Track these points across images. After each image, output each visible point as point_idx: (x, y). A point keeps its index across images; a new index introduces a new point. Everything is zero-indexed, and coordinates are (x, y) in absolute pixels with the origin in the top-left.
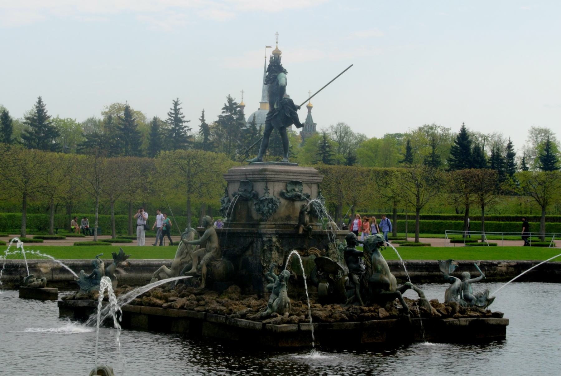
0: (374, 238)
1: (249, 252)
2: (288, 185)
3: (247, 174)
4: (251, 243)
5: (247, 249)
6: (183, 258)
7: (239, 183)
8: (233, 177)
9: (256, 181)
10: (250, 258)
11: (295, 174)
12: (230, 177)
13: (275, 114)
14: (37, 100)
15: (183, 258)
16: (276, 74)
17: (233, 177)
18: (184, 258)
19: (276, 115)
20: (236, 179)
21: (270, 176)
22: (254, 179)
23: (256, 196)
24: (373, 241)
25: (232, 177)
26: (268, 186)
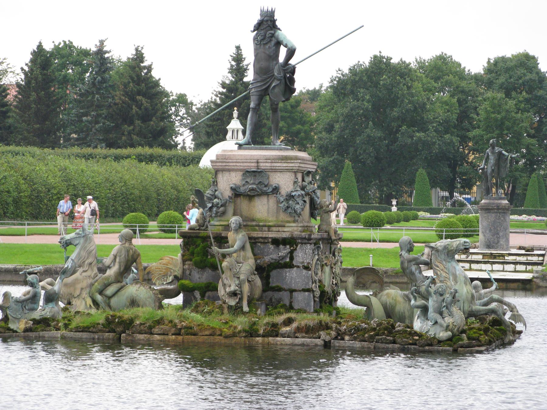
0: (458, 243)
2: (305, 175)
3: (260, 161)
6: (84, 271)
9: (275, 171)
11: (305, 162)
12: (224, 164)
13: (273, 85)
14: (234, 50)
16: (272, 32)
18: (86, 271)
19: (275, 86)
20: (236, 167)
21: (264, 164)
22: (272, 168)
24: (454, 246)
25: (227, 164)
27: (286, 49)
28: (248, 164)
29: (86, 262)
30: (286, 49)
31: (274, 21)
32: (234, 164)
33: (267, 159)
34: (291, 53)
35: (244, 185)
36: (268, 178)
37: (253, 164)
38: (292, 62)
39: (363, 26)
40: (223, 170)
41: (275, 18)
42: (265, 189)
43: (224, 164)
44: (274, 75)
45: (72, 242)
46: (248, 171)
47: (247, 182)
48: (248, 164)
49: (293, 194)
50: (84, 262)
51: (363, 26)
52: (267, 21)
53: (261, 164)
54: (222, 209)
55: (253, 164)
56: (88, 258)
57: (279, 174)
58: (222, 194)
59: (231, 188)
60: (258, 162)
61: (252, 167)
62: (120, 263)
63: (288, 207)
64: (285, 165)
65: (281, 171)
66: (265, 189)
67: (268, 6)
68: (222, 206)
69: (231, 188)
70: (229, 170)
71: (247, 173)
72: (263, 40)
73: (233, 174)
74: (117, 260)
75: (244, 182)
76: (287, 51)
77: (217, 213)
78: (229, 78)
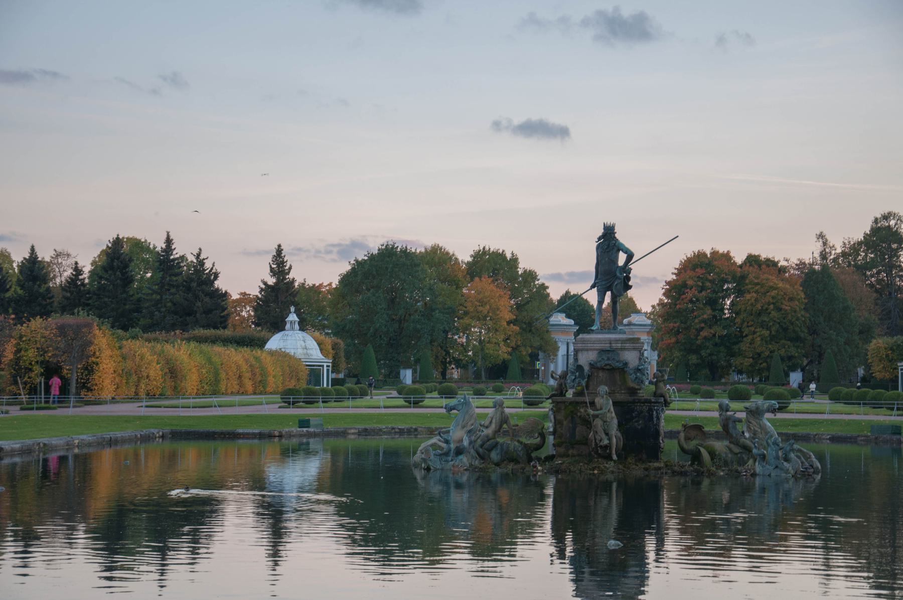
0: (768, 404)
7: (596, 353)
8: (589, 345)
9: (623, 349)
20: (593, 348)
27: (626, 255)
29: (469, 424)
30: (626, 255)
32: (592, 345)
33: (617, 341)
34: (630, 256)
35: (600, 361)
37: (607, 345)
39: (677, 237)
40: (582, 350)
42: (617, 364)
43: (584, 345)
44: (616, 275)
45: (456, 408)
46: (603, 351)
47: (603, 359)
49: (640, 368)
51: (677, 237)
53: (613, 345)
55: (607, 345)
57: (627, 353)
59: (590, 364)
61: (606, 346)
62: (496, 423)
63: (636, 378)
64: (632, 345)
65: (628, 349)
67: (609, 221)
69: (590, 364)
70: (587, 350)
71: (602, 351)
73: (590, 353)
74: (494, 421)
75: (600, 359)
76: (627, 257)
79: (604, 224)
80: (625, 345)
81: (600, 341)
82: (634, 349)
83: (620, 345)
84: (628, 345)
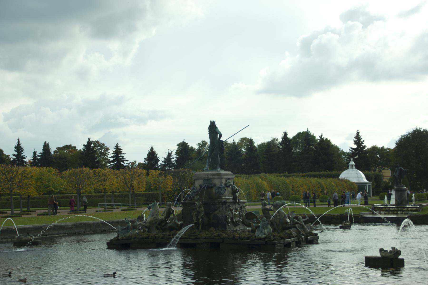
0: (281, 202)
1: (218, 211)
4: (219, 207)
5: (216, 210)
7: (202, 180)
8: (199, 177)
10: (218, 214)
12: (197, 177)
15: (154, 218)
16: (215, 129)
17: (199, 177)
23: (215, 185)
26: (222, 181)
28: (205, 177)
29: (155, 214)
31: (215, 125)
34: (221, 136)
36: (212, 181)
37: (207, 177)
38: (221, 139)
39: (249, 125)
40: (197, 179)
41: (216, 124)
42: (211, 185)
43: (197, 177)
48: (205, 177)
50: (154, 214)
51: (249, 125)
52: (212, 125)
53: (209, 177)
54: (196, 193)
55: (207, 177)
56: (156, 213)
57: (215, 180)
58: (196, 188)
59: (199, 185)
60: (208, 176)
61: (206, 177)
63: (219, 192)
64: (217, 176)
66: (211, 185)
67: (213, 120)
68: (196, 192)
70: (199, 179)
71: (205, 180)
72: (211, 132)
73: (200, 180)
77: (195, 195)
78: (17, 143)
79: (211, 121)
80: (214, 176)
81: (204, 175)
82: (219, 178)
83: (212, 177)
84: (215, 176)
